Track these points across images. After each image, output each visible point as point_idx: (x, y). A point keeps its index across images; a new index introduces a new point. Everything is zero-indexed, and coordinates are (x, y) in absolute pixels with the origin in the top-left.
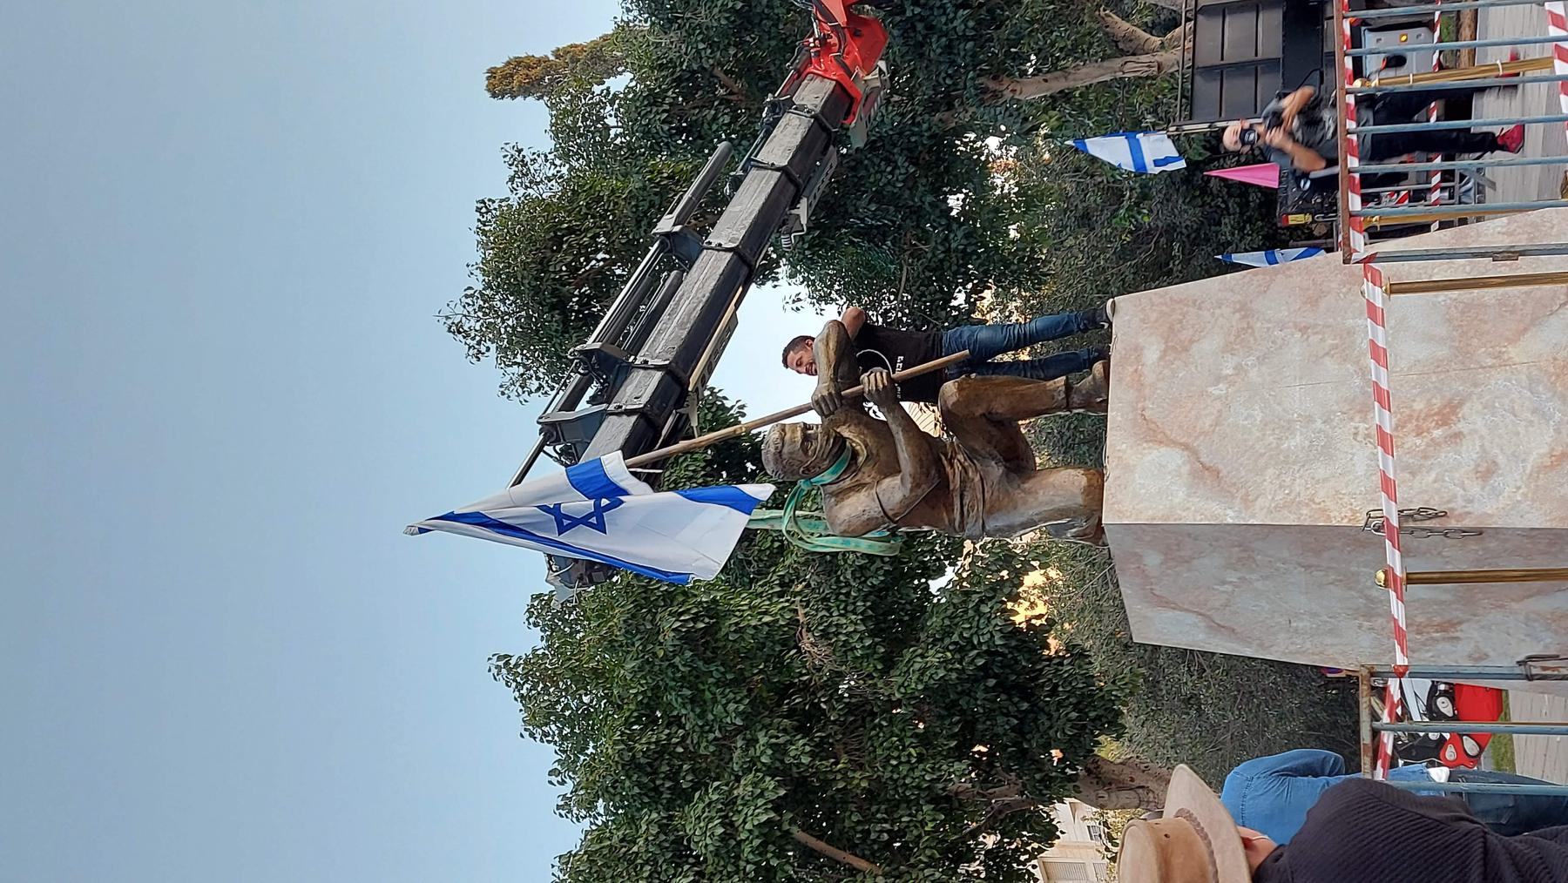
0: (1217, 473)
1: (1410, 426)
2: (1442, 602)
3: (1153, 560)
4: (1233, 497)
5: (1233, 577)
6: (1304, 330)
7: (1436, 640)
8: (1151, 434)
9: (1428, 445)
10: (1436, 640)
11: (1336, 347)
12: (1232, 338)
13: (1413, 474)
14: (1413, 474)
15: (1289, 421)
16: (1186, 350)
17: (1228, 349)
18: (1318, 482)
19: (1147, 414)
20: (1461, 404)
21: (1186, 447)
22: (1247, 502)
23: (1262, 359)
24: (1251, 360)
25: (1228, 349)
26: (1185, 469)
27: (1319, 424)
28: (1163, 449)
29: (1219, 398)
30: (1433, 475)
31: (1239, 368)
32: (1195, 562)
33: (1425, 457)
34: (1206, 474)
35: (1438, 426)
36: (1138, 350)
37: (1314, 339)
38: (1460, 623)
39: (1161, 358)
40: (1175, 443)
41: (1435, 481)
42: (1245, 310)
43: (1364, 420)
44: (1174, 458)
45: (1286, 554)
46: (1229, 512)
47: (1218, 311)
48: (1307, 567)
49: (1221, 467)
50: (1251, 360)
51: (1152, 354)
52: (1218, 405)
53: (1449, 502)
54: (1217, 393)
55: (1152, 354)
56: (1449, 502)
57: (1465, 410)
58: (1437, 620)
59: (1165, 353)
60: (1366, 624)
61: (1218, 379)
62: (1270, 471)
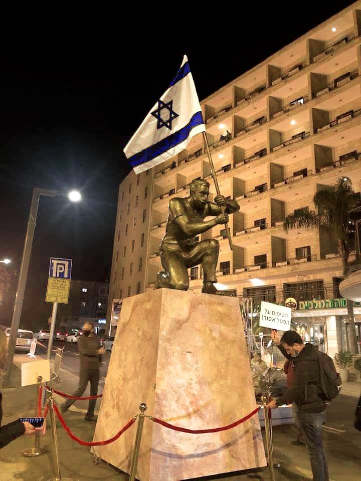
0: (178, 329)
1: (193, 400)
2: (126, 405)
3: (148, 306)
4: (170, 335)
5: (140, 333)
6: (227, 361)
7: (114, 401)
8: (194, 306)
9: (186, 406)
10: (114, 401)
11: (221, 372)
15: (196, 355)
16: (221, 320)
17: (221, 334)
19: (200, 306)
20: (201, 418)
21: (188, 319)
22: (169, 340)
23: (217, 347)
24: (217, 343)
25: (221, 334)
26: (181, 318)
27: (195, 366)
29: (205, 331)
31: (214, 339)
32: (146, 320)
33: (183, 405)
34: (179, 325)
35: (193, 409)
36: (222, 304)
37: (224, 364)
38: (119, 411)
39: (219, 311)
40: (190, 314)
42: (233, 342)
43: (196, 383)
45: (147, 353)
46: (165, 333)
48: (142, 360)
50: (217, 343)
51: (220, 309)
52: (203, 330)
53: (166, 415)
54: (207, 329)
55: (220, 309)
57: (199, 420)
58: (120, 403)
59: (220, 313)
60: (121, 378)
61: (211, 331)
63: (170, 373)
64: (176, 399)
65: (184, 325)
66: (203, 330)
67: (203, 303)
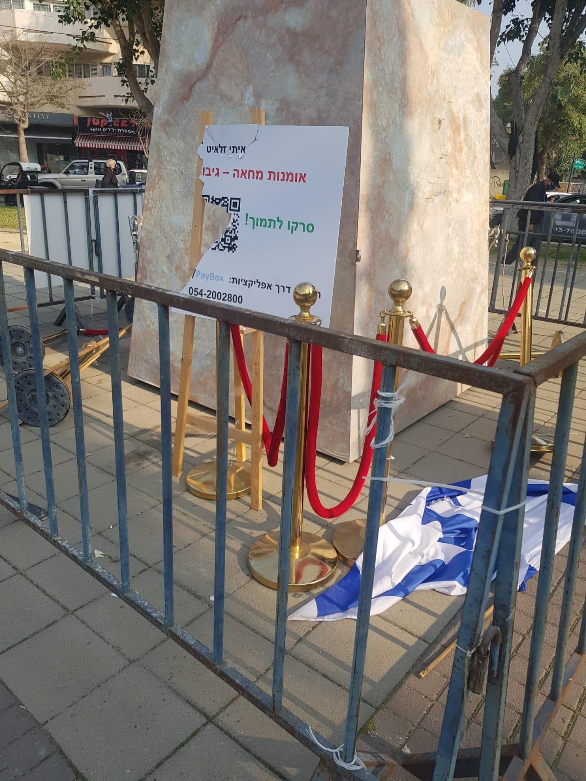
0: (186, 98)
9: (184, 272)
12: (293, 109)
13: (169, 257)
14: (169, 257)
16: (291, 58)
18: (172, 185)
19: (241, 23)
21: (209, 67)
26: (193, 68)
28: (210, 44)
30: (166, 271)
33: (177, 268)
34: (188, 86)
41: (162, 271)
44: (201, 57)
46: (160, 111)
47: (324, 91)
49: (191, 101)
52: (237, 97)
53: (151, 278)
56: (151, 278)
61: (258, 96)
62: (182, 145)
63: (163, 199)
64: (168, 252)
65: (198, 85)
66: (237, 97)
67: (250, 13)
